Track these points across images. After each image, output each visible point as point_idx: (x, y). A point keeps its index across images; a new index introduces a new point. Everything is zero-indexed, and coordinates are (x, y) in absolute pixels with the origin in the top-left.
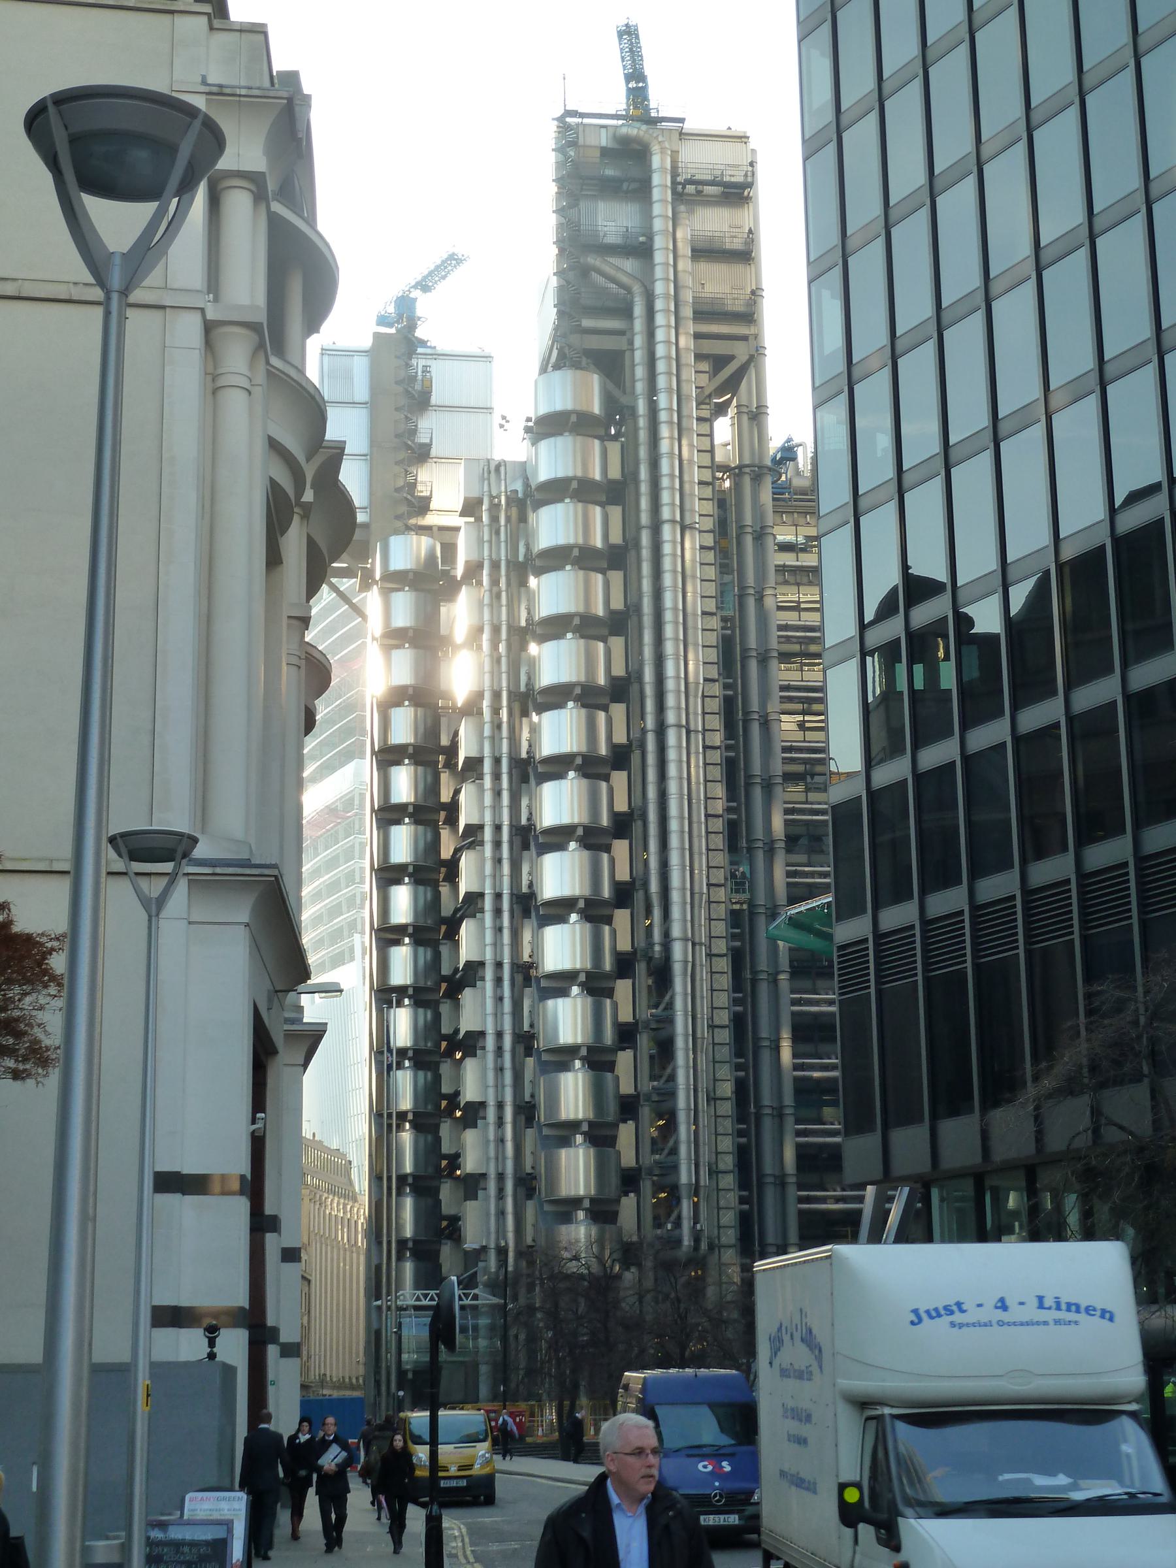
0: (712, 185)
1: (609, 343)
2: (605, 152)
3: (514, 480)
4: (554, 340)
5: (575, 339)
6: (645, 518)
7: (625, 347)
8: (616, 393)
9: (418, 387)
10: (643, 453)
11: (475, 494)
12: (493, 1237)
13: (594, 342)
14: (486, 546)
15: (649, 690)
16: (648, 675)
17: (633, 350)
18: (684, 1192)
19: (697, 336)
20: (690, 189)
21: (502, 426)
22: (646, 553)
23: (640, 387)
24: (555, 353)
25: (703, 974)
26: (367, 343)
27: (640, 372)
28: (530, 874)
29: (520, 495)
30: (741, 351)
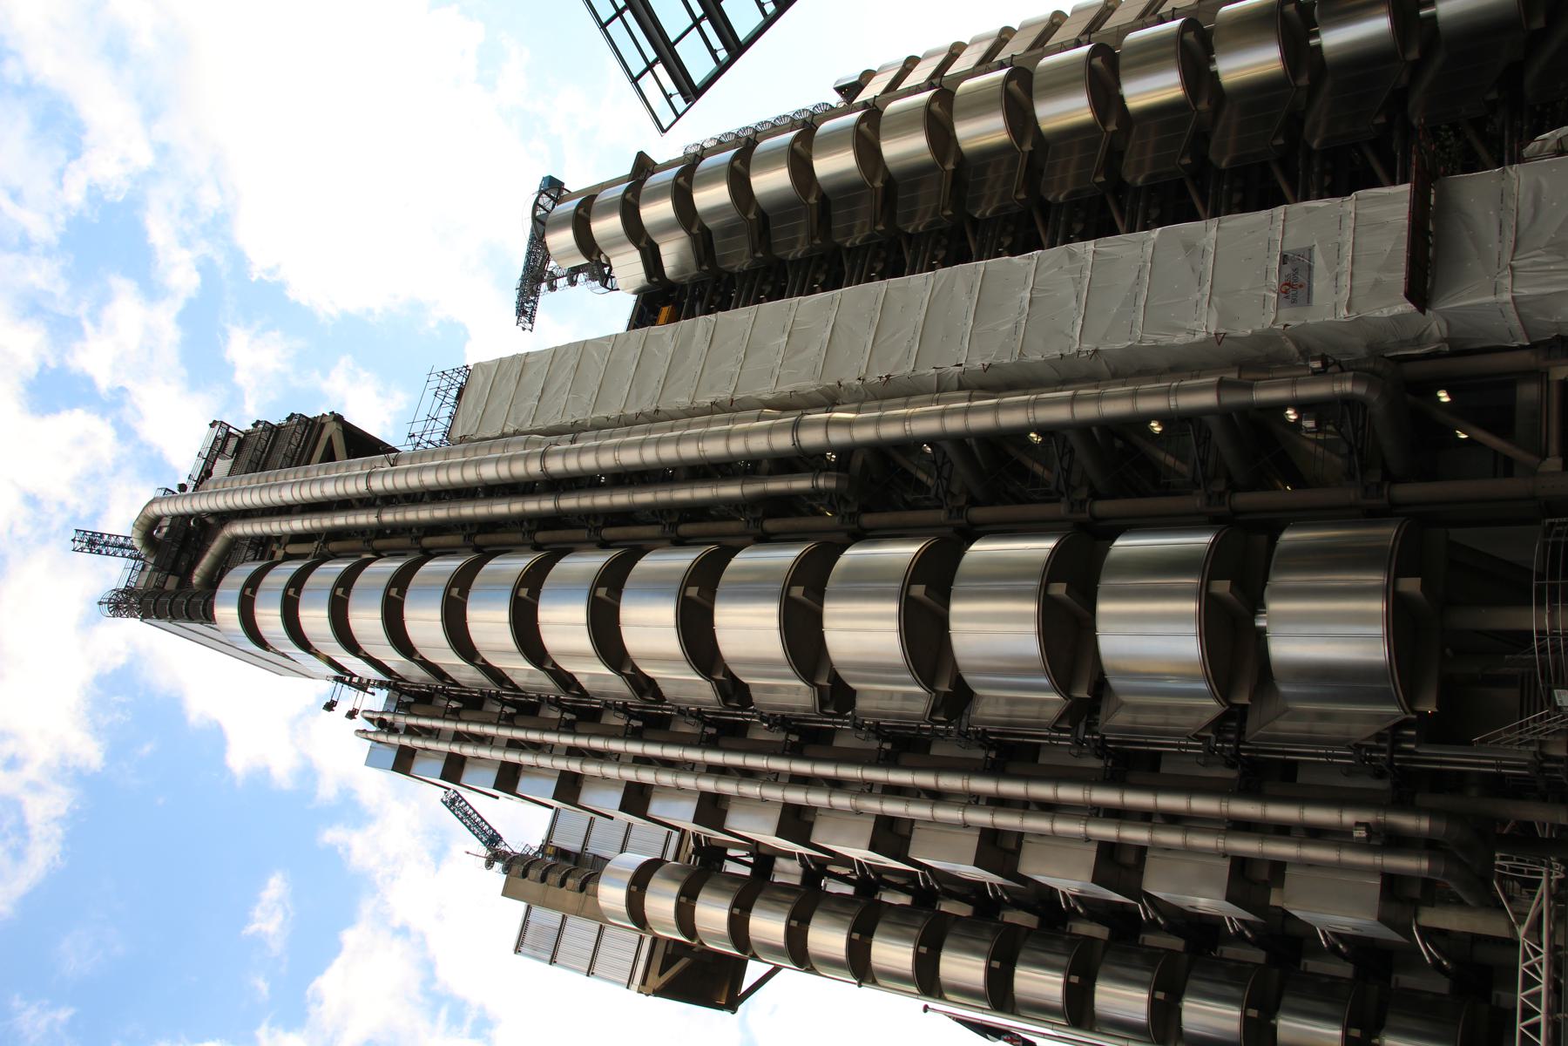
0: (214, 463)
12: (1350, 857)
18: (1235, 398)
26: (519, 907)
30: (331, 429)
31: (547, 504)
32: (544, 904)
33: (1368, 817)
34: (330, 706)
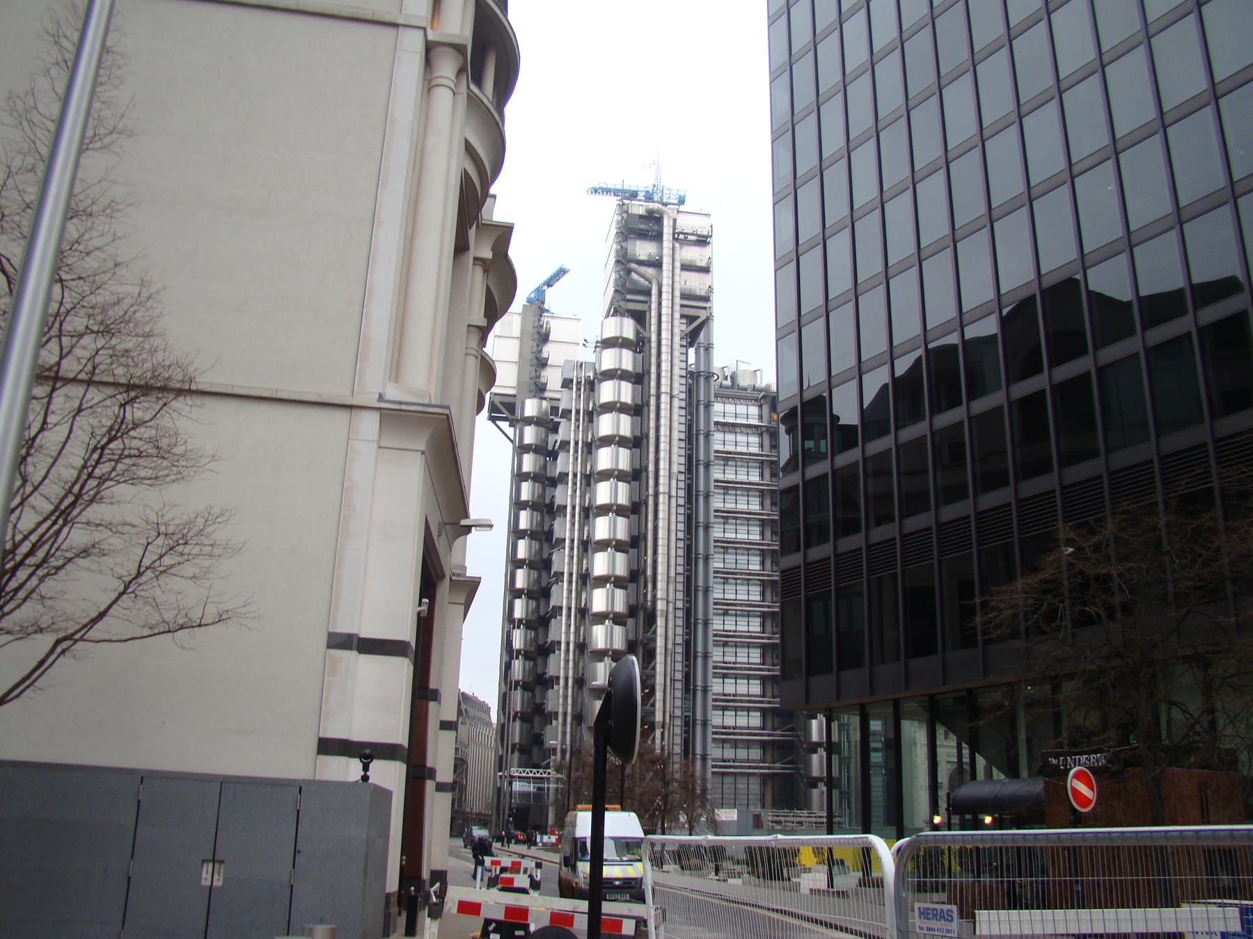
1: (639, 307)
2: (641, 217)
3: (589, 371)
4: (612, 304)
5: (622, 304)
6: (653, 391)
7: (646, 309)
8: (641, 330)
9: (544, 331)
10: (653, 359)
11: (568, 376)
13: (632, 306)
14: (574, 402)
15: (651, 475)
16: (651, 468)
17: (650, 311)
19: (682, 306)
20: (681, 237)
21: (584, 345)
22: (653, 408)
23: (654, 328)
24: (612, 310)
25: (671, 616)
27: (654, 321)
28: (587, 564)
29: (592, 378)
30: (703, 315)
31: (651, 491)
32: (523, 331)
33: (569, 747)
34: (585, 340)
